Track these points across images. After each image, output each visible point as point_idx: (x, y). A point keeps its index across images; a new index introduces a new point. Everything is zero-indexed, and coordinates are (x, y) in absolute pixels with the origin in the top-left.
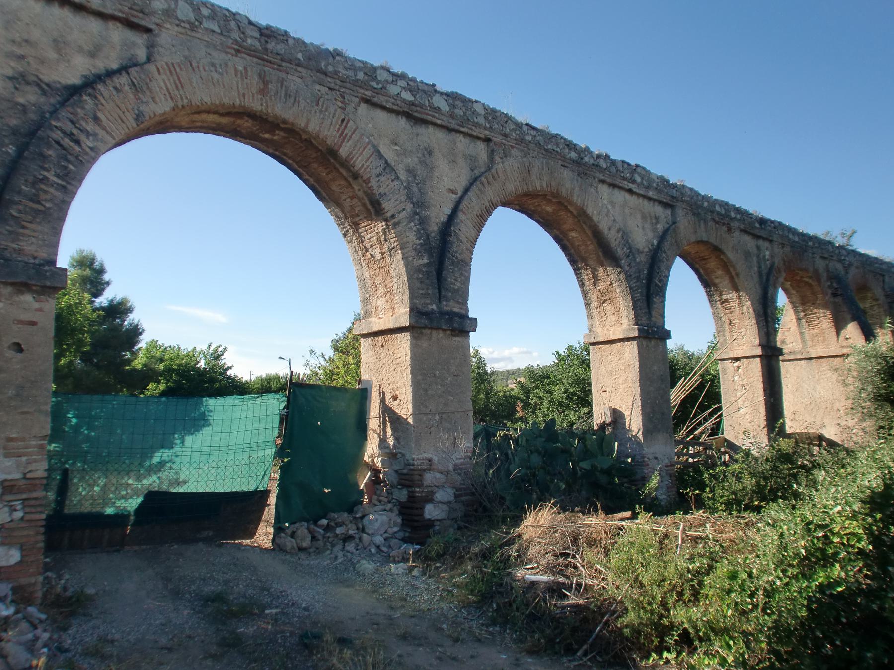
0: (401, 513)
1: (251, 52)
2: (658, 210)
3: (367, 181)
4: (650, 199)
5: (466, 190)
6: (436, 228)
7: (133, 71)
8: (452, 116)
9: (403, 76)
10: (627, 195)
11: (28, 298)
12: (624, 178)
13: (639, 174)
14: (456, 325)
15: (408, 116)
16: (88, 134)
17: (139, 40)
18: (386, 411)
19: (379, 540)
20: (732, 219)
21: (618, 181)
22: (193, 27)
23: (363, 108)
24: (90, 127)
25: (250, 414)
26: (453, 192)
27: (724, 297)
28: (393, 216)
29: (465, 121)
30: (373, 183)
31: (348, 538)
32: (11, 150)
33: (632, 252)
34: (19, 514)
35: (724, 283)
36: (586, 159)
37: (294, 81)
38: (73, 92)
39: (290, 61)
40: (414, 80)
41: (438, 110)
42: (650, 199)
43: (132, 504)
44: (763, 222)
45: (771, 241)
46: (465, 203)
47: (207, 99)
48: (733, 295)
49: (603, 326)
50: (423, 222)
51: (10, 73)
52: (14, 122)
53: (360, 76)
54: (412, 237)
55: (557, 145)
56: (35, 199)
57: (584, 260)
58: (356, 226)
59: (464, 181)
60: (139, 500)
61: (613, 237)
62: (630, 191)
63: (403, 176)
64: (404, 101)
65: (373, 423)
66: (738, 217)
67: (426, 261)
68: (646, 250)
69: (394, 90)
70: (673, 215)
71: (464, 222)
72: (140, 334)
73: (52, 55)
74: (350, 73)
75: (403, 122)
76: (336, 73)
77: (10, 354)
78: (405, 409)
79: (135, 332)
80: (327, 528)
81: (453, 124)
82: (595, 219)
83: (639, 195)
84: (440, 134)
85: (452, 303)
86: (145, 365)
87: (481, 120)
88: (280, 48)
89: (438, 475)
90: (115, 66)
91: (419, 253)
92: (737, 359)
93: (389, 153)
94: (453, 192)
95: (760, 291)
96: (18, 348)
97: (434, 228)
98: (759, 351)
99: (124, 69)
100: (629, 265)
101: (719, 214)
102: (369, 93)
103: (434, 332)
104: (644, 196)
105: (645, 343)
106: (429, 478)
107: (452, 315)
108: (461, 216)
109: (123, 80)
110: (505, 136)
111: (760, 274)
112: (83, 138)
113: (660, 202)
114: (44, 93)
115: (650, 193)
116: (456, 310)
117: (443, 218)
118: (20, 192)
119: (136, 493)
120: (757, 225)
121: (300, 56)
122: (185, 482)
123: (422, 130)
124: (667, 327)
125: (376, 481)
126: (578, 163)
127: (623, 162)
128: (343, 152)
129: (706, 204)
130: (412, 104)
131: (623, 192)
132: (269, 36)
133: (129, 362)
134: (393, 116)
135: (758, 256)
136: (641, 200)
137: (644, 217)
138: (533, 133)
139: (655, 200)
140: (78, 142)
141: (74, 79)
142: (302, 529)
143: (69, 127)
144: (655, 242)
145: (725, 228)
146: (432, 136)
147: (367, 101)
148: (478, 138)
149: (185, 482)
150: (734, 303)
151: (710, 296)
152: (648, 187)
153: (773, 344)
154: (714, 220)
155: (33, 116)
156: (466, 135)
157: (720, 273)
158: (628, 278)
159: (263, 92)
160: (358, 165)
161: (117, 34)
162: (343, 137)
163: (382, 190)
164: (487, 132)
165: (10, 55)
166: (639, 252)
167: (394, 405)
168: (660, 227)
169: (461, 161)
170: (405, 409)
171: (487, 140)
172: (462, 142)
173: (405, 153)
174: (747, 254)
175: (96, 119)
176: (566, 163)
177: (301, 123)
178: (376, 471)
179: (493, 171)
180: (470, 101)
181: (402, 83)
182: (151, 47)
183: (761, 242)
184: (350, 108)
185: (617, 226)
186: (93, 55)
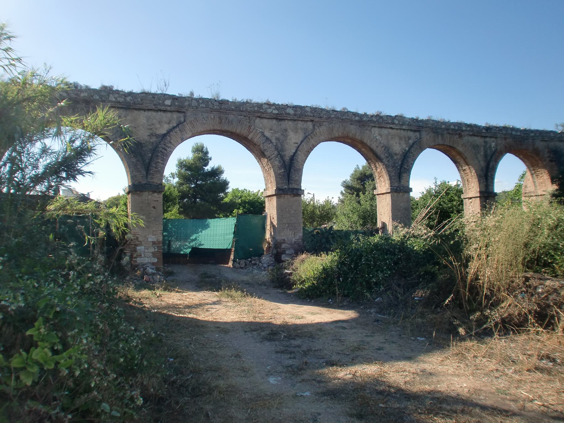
0: (275, 257)
1: (216, 110)
2: (411, 134)
3: (259, 146)
4: (404, 130)
5: (302, 142)
6: (288, 158)
7: (180, 126)
8: (295, 115)
9: (274, 104)
10: (390, 130)
11: (156, 194)
12: (387, 123)
13: (397, 120)
14: (294, 193)
15: (276, 119)
16: (169, 147)
17: (182, 115)
18: (271, 223)
19: (265, 265)
20: (463, 131)
21: (383, 125)
22: (197, 108)
23: (258, 120)
24: (169, 145)
25: (223, 224)
26: (296, 143)
27: (464, 168)
28: (269, 157)
29: (301, 115)
30: (261, 146)
31: (255, 264)
32: (150, 155)
33: (390, 155)
34: (156, 250)
35: (462, 162)
36: (365, 119)
37: (231, 117)
38: (164, 136)
39: (229, 110)
40: (278, 105)
41: (289, 114)
42: (404, 130)
43: (188, 251)
44: (488, 129)
45: (496, 138)
46: (301, 147)
47: (202, 130)
48: (466, 167)
49: (381, 187)
50: (282, 157)
51: (149, 134)
52: (150, 147)
53: (256, 109)
54: (277, 163)
55: (348, 116)
56: (156, 168)
57: (370, 159)
58: (260, 159)
59: (301, 139)
60: (190, 250)
61: (379, 151)
62: (391, 128)
63: (274, 141)
64: (274, 114)
65: (268, 227)
66: (468, 129)
67: (283, 171)
68: (401, 153)
69: (269, 111)
70: (420, 135)
71: (300, 155)
72: (228, 184)
73: (158, 126)
74: (252, 109)
75: (274, 121)
76: (246, 110)
77: (152, 209)
78: (275, 223)
79: (225, 184)
80: (251, 262)
81: (296, 118)
82: (368, 144)
83: (397, 129)
84: (290, 123)
85: (294, 185)
86: (231, 200)
87: (309, 114)
88: (226, 106)
89: (287, 245)
90: (175, 125)
91: (280, 169)
92: (471, 198)
93: (267, 134)
94: (296, 143)
95: (483, 164)
96: (154, 207)
97: (287, 158)
98: (478, 195)
99: (178, 125)
100: (388, 161)
101: (452, 129)
102: (259, 114)
103: (286, 196)
104: (401, 129)
105: (395, 194)
106: (283, 246)
107: (293, 189)
108: (299, 153)
109: (177, 129)
110: (321, 117)
111: (486, 156)
112: (167, 148)
113: (411, 130)
114: (157, 138)
115: (404, 127)
116: (296, 187)
117: (292, 154)
118: (152, 166)
119: (189, 247)
120: (484, 131)
121: (233, 107)
122: (203, 245)
123: (282, 122)
124: (410, 187)
125: (269, 248)
126: (359, 121)
127: (387, 116)
128: (250, 137)
129: (443, 126)
130: (278, 114)
131: (387, 129)
132: (222, 104)
133: (223, 198)
134: (270, 120)
135: (485, 147)
136: (399, 131)
137: (401, 138)
138: (335, 113)
139: (407, 130)
140: (166, 150)
141: (164, 132)
142: (243, 262)
143: (163, 146)
144: (407, 149)
145: (457, 136)
146: (288, 124)
147: (259, 117)
148: (308, 121)
149: (203, 245)
150: (468, 171)
151: (458, 168)
152: (403, 125)
153: (490, 191)
154: (449, 133)
155: (154, 145)
156: (302, 121)
157: (458, 157)
158: (387, 167)
159: (220, 123)
160: (255, 140)
161: (175, 115)
162: (250, 132)
163: (265, 148)
164: (311, 118)
165: (148, 129)
166: (396, 154)
167: (273, 220)
168: (411, 142)
169: (300, 131)
170: (275, 223)
171: (312, 121)
172: (300, 124)
173: (275, 132)
174: (475, 147)
175: (171, 143)
176: (352, 122)
177: (234, 130)
178: (269, 243)
179: (314, 133)
180: (304, 107)
181: (274, 107)
182: (185, 117)
183: (488, 139)
184: (252, 122)
185: (382, 145)
186: (169, 123)
